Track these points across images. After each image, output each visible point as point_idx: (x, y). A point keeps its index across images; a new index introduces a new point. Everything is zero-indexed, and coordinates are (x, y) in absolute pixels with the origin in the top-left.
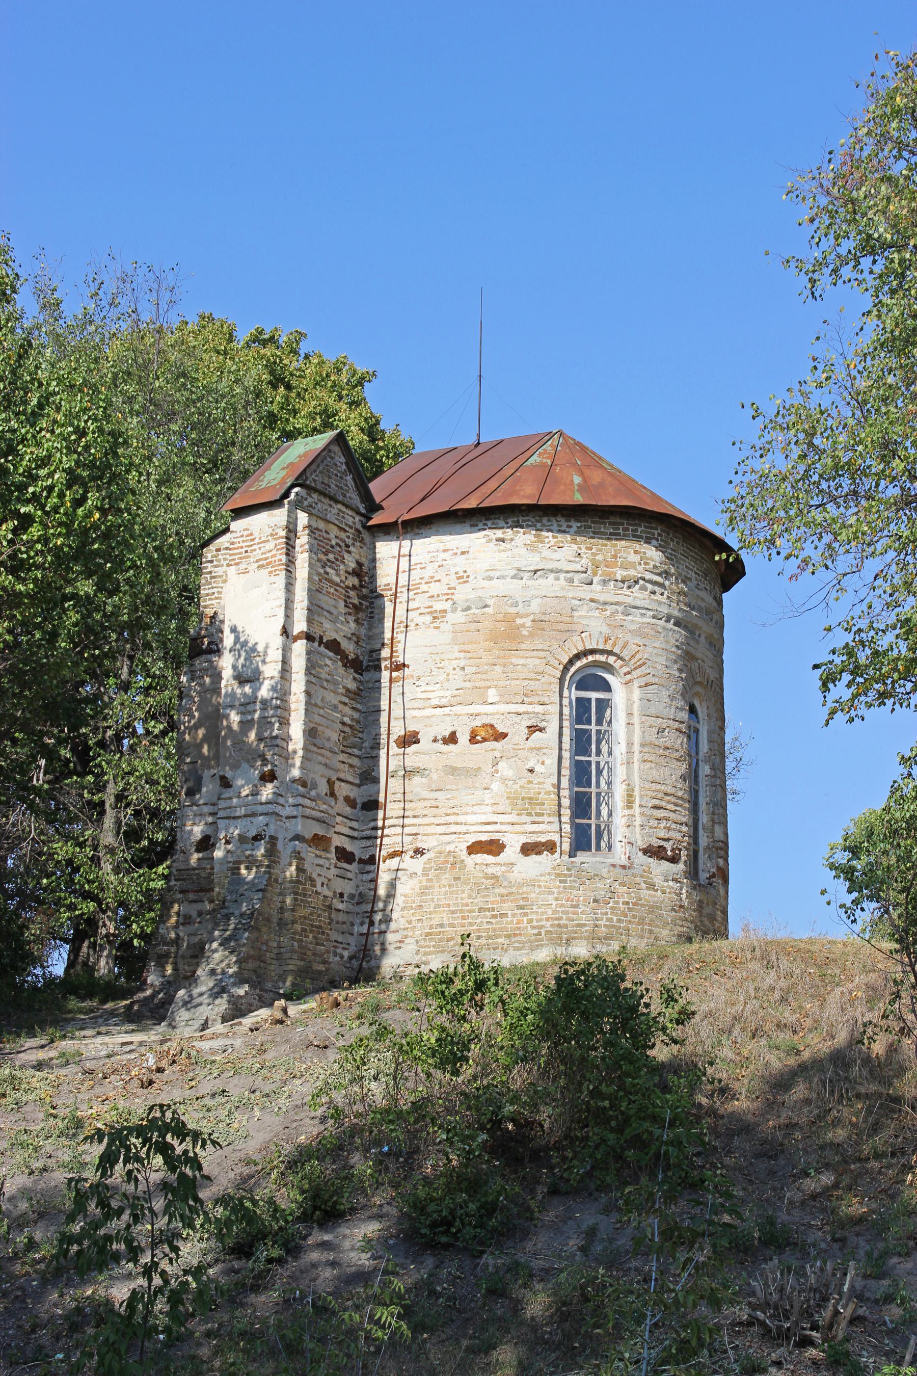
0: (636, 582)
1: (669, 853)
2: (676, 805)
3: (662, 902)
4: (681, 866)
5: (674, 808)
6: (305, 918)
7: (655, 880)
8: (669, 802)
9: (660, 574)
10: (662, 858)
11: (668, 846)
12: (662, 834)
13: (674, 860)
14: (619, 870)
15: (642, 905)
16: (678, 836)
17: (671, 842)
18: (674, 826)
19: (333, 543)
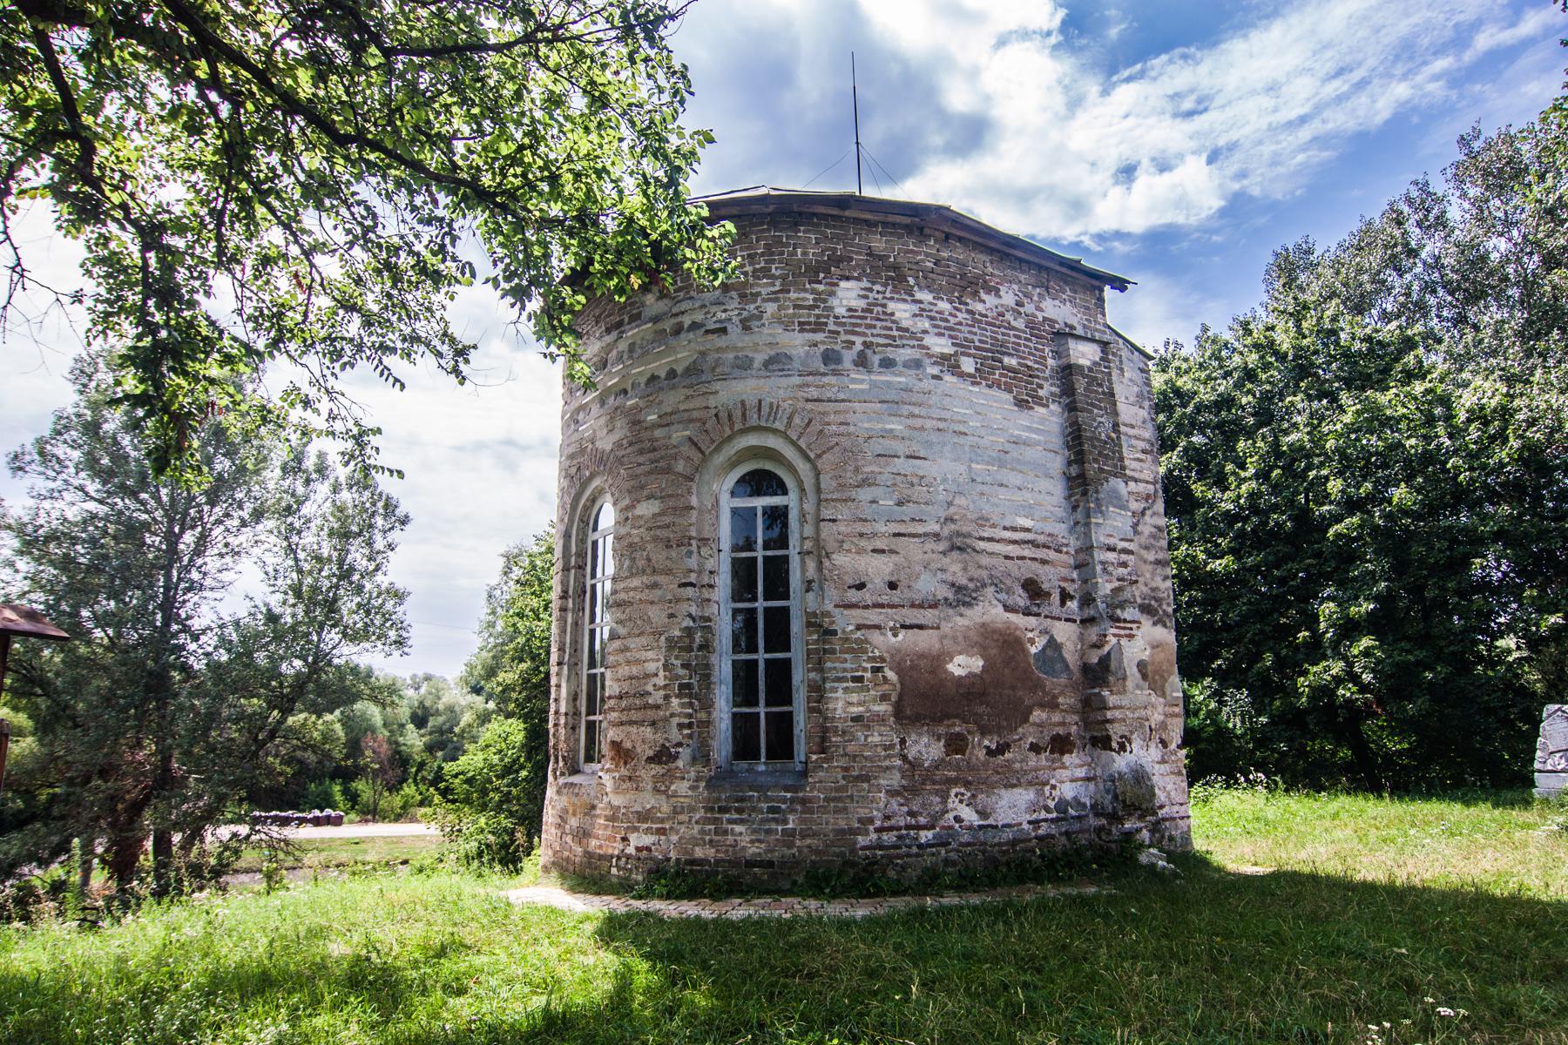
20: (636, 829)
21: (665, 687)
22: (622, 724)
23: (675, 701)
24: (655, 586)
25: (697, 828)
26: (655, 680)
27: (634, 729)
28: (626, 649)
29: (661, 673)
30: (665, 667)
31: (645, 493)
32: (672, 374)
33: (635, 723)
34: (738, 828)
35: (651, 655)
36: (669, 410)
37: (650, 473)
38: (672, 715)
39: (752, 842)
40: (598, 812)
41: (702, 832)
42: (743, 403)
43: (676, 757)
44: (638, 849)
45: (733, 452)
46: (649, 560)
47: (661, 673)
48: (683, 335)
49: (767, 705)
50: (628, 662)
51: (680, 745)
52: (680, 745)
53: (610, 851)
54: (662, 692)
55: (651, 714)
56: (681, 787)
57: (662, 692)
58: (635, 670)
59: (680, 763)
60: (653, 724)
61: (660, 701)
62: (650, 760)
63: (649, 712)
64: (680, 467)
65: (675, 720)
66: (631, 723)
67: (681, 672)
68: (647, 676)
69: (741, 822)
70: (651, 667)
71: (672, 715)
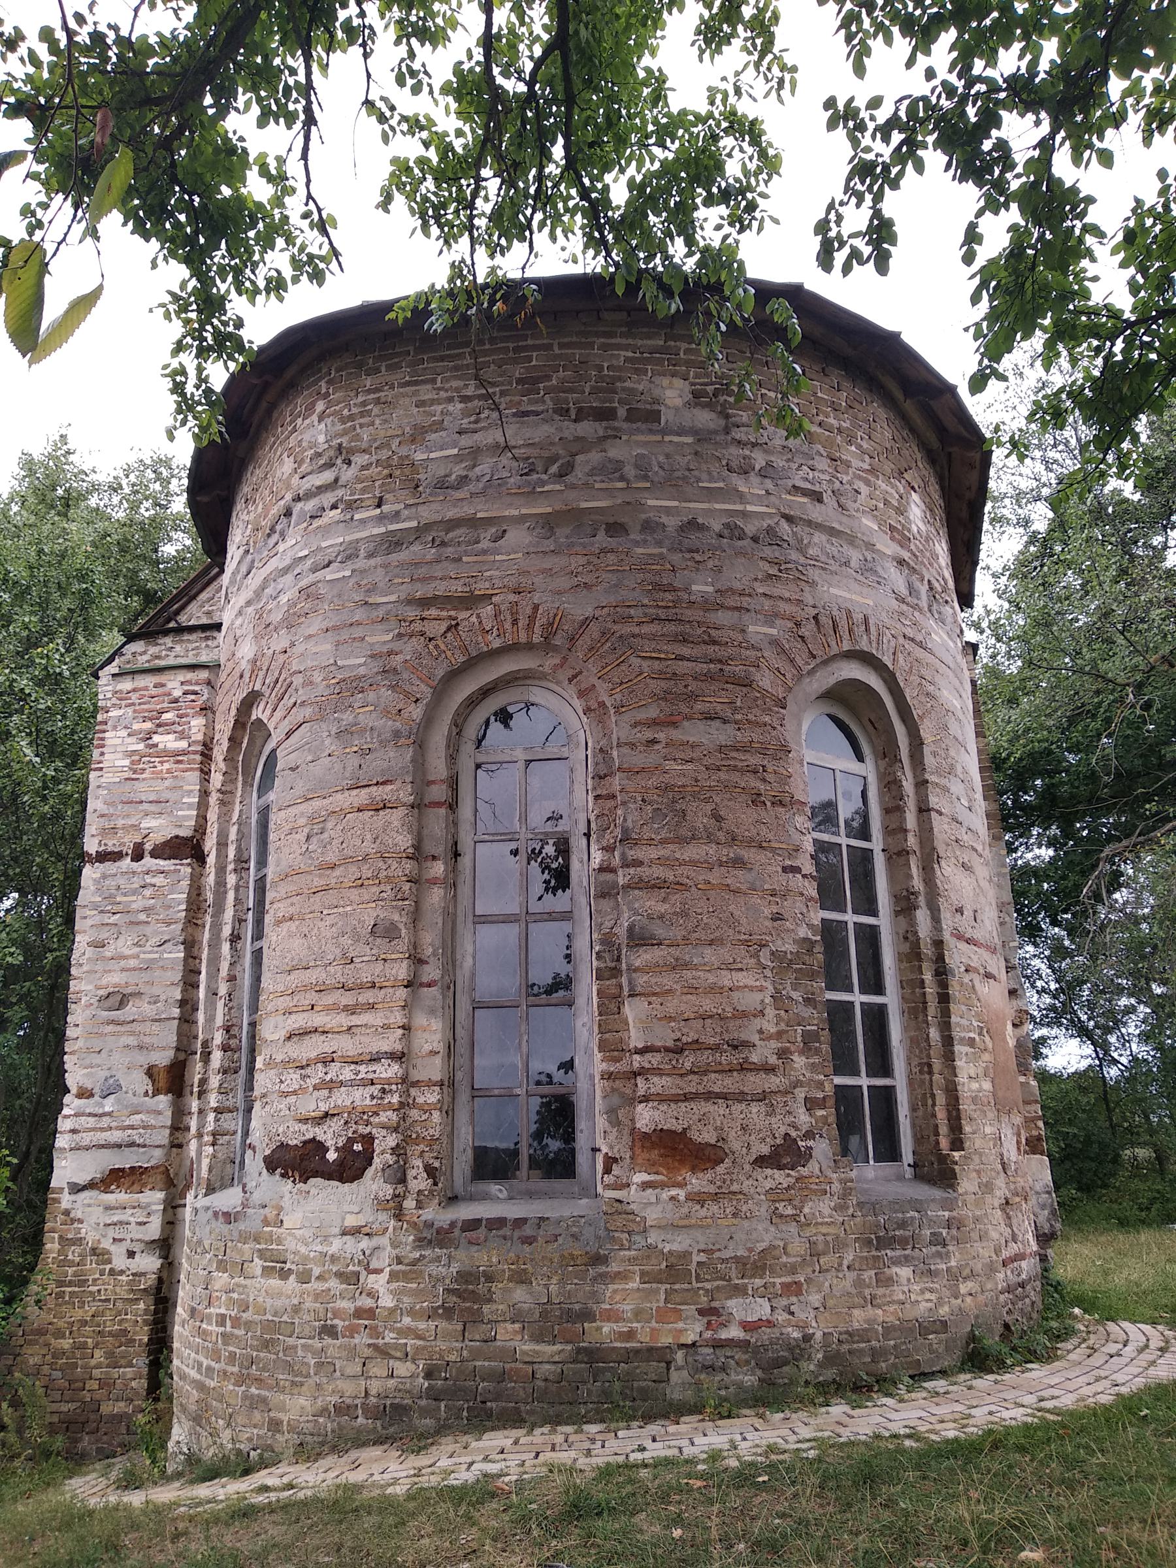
0: (288, 513)
1: (332, 1156)
2: (351, 1010)
3: (296, 1309)
4: (373, 1184)
5: (345, 1020)
6: (84, 1323)
7: (291, 1244)
8: (328, 1009)
9: (330, 465)
10: (316, 1174)
11: (331, 1136)
12: (312, 1104)
13: (350, 1167)
14: (220, 1226)
15: (248, 1325)
16: (361, 1097)
17: (336, 1125)
18: (347, 1073)
19: (177, 693)
20: (740, 1291)
21: (779, 1035)
22: (686, 1098)
23: (799, 1061)
24: (738, 863)
25: (851, 1276)
26: (757, 1023)
27: (717, 1110)
28: (679, 965)
29: (770, 1012)
30: (777, 998)
31: (699, 706)
32: (733, 532)
33: (724, 1097)
34: (904, 1272)
35: (743, 979)
36: (737, 585)
37: (709, 677)
38: (797, 1084)
39: (922, 1292)
40: (614, 1267)
41: (859, 1283)
42: (849, 614)
43: (804, 1157)
44: (746, 1326)
45: (832, 681)
46: (718, 818)
47: (770, 1012)
48: (754, 479)
49: (856, 1073)
50: (692, 990)
51: (809, 1135)
52: (809, 1135)
53: (666, 1340)
54: (774, 1044)
55: (755, 1082)
56: (822, 1208)
57: (774, 1044)
58: (708, 1004)
59: (813, 1167)
60: (762, 1097)
61: (773, 1060)
62: (761, 1161)
63: (751, 1077)
64: (765, 680)
65: (800, 1093)
66: (710, 1096)
67: (807, 1012)
68: (744, 1015)
69: (907, 1260)
70: (750, 1001)
71: (797, 1084)
